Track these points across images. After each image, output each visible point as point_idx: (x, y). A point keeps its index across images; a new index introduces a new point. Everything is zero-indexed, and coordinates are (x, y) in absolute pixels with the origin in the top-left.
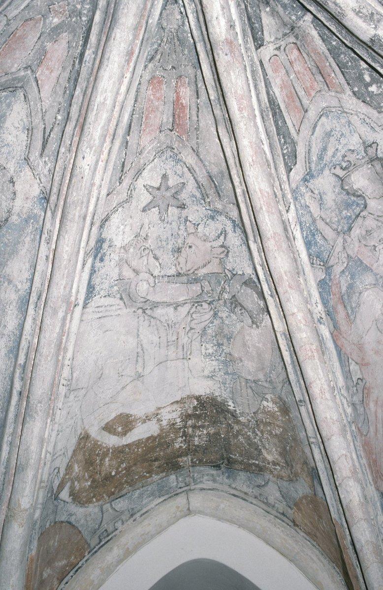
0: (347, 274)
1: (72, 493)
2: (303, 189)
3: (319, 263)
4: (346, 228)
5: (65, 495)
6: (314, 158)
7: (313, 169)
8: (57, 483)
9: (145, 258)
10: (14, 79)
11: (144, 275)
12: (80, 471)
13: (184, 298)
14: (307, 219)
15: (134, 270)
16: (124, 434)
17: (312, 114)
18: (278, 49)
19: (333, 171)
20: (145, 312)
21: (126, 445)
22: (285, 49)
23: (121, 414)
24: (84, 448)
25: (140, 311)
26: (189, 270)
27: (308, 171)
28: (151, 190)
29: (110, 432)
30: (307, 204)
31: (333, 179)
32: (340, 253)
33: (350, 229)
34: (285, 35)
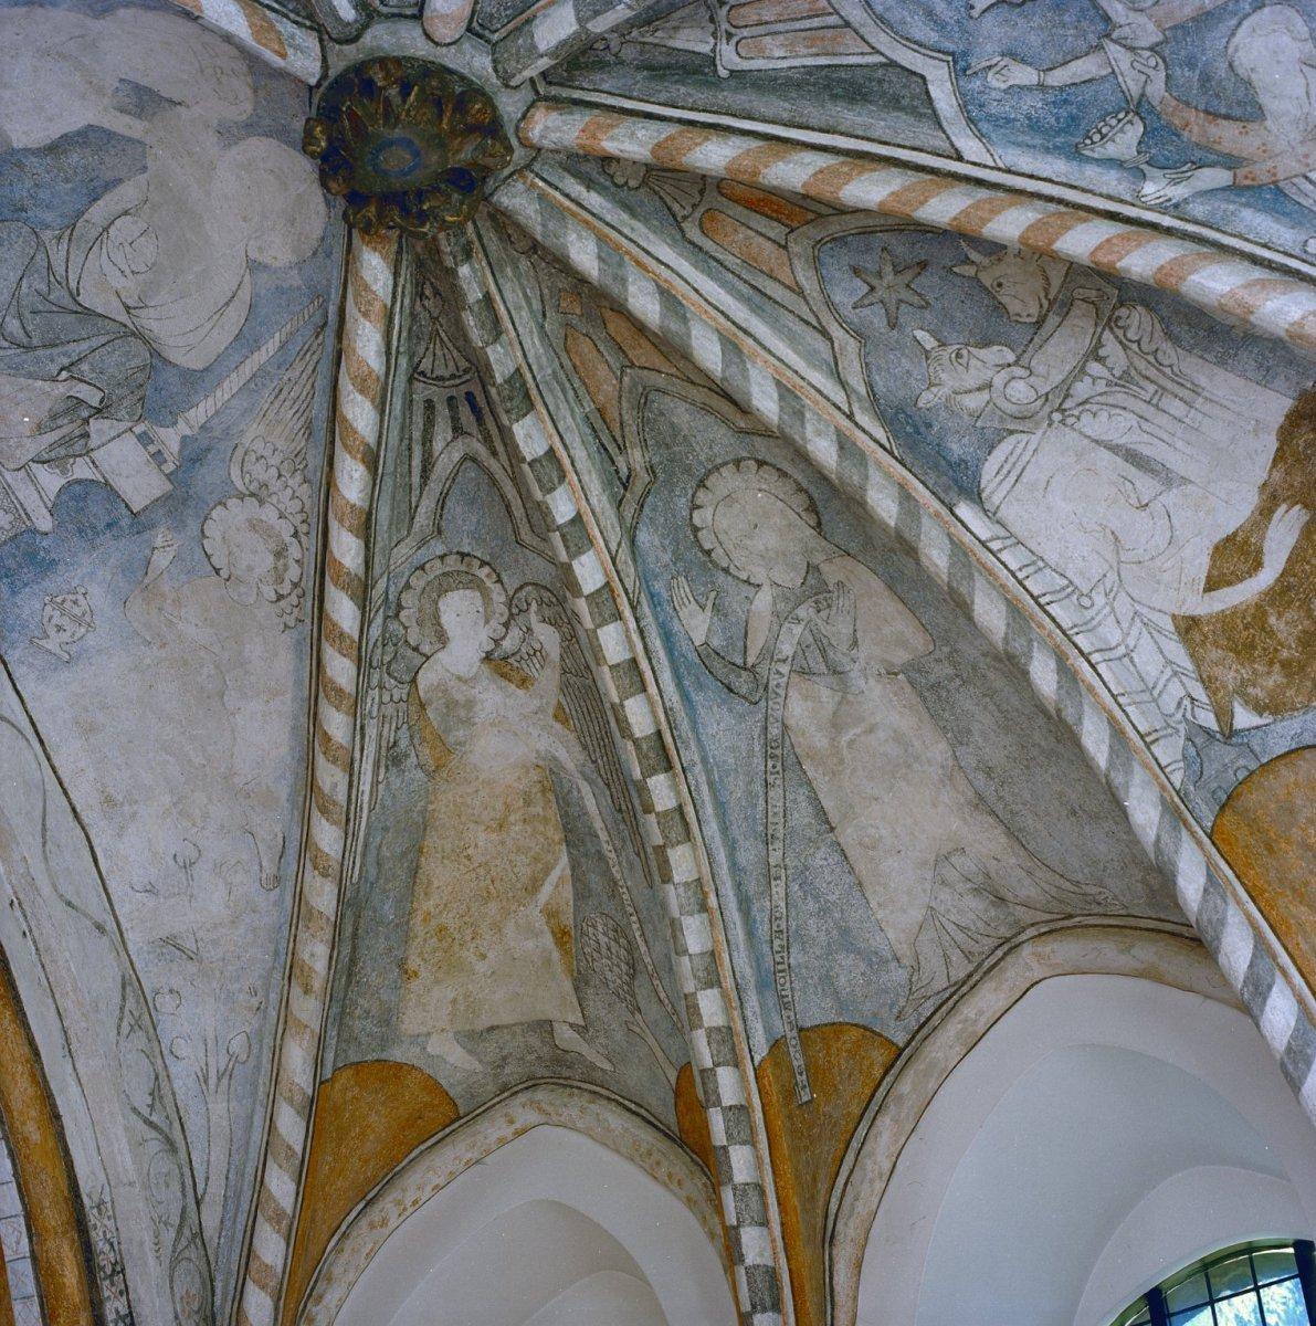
0: (1178, 71)
1: (1259, 709)
2: (977, 84)
3: (1114, 122)
4: (1101, 26)
5: (1243, 718)
7: (951, 47)
8: (1208, 719)
9: (973, 362)
10: (630, 392)
11: (998, 381)
12: (1237, 671)
13: (1088, 341)
14: (1031, 103)
15: (979, 389)
16: (1258, 565)
18: (729, 36)
19: (975, 13)
20: (1065, 410)
21: (1282, 575)
22: (735, 27)
23: (1216, 548)
24: (1206, 638)
25: (1057, 416)
26: (1041, 306)
27: (950, 58)
28: (866, 302)
29: (1229, 584)
30: (1004, 86)
31: (989, 17)
32: (1135, 64)
33: (1107, 19)
34: (712, 20)
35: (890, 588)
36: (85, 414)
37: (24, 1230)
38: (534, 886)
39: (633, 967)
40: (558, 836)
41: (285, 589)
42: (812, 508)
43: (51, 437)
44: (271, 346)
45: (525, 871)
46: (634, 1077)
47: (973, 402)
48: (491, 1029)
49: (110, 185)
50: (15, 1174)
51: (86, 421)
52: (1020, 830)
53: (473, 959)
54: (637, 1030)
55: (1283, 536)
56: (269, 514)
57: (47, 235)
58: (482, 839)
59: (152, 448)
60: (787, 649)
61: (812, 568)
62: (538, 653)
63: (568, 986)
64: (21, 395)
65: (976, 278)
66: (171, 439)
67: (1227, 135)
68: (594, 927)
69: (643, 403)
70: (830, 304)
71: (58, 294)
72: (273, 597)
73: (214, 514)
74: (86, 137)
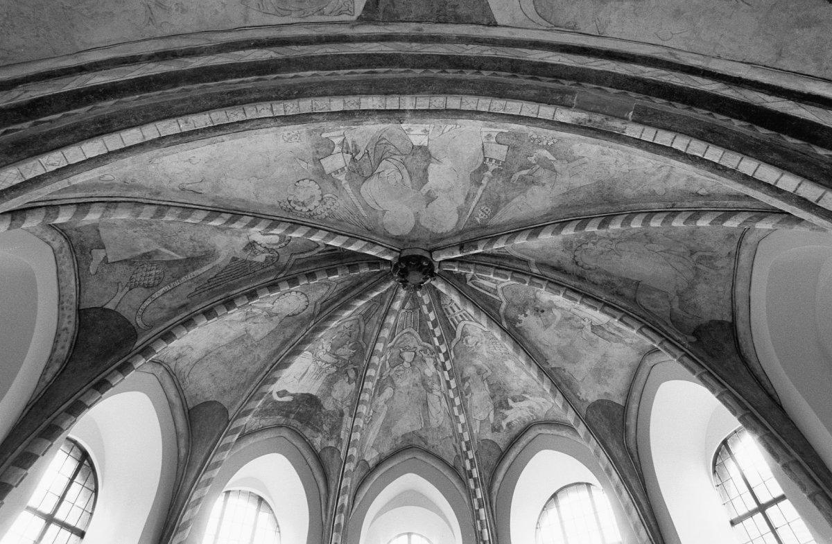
6: (398, 342)
17: (404, 331)
35: (272, 331)
36: (354, 154)
37: (61, 166)
38: (166, 247)
39: (148, 287)
40: (189, 255)
41: (294, 205)
42: (294, 315)
43: (350, 145)
44: (363, 213)
45: (174, 245)
46: (93, 285)
47: (320, 347)
48: (98, 231)
49: (411, 177)
50: (90, 159)
51: (352, 154)
52: (202, 362)
53: (135, 230)
54: (120, 288)
55: (287, 399)
56: (316, 203)
57: (404, 157)
58: (188, 236)
59: (339, 171)
60: (254, 310)
61: (277, 315)
62: (255, 254)
63: (126, 257)
64: (365, 140)
65: (346, 344)
66: (342, 177)
67: (377, 393)
68: (157, 269)
69: (326, 284)
70: (344, 322)
71: (388, 155)
72: (290, 199)
73: (317, 185)
74: (424, 180)
